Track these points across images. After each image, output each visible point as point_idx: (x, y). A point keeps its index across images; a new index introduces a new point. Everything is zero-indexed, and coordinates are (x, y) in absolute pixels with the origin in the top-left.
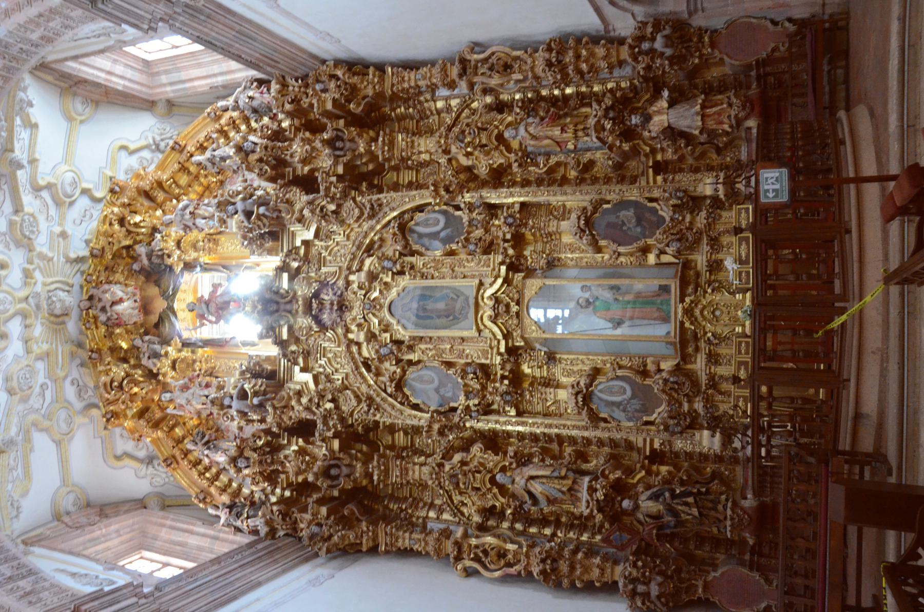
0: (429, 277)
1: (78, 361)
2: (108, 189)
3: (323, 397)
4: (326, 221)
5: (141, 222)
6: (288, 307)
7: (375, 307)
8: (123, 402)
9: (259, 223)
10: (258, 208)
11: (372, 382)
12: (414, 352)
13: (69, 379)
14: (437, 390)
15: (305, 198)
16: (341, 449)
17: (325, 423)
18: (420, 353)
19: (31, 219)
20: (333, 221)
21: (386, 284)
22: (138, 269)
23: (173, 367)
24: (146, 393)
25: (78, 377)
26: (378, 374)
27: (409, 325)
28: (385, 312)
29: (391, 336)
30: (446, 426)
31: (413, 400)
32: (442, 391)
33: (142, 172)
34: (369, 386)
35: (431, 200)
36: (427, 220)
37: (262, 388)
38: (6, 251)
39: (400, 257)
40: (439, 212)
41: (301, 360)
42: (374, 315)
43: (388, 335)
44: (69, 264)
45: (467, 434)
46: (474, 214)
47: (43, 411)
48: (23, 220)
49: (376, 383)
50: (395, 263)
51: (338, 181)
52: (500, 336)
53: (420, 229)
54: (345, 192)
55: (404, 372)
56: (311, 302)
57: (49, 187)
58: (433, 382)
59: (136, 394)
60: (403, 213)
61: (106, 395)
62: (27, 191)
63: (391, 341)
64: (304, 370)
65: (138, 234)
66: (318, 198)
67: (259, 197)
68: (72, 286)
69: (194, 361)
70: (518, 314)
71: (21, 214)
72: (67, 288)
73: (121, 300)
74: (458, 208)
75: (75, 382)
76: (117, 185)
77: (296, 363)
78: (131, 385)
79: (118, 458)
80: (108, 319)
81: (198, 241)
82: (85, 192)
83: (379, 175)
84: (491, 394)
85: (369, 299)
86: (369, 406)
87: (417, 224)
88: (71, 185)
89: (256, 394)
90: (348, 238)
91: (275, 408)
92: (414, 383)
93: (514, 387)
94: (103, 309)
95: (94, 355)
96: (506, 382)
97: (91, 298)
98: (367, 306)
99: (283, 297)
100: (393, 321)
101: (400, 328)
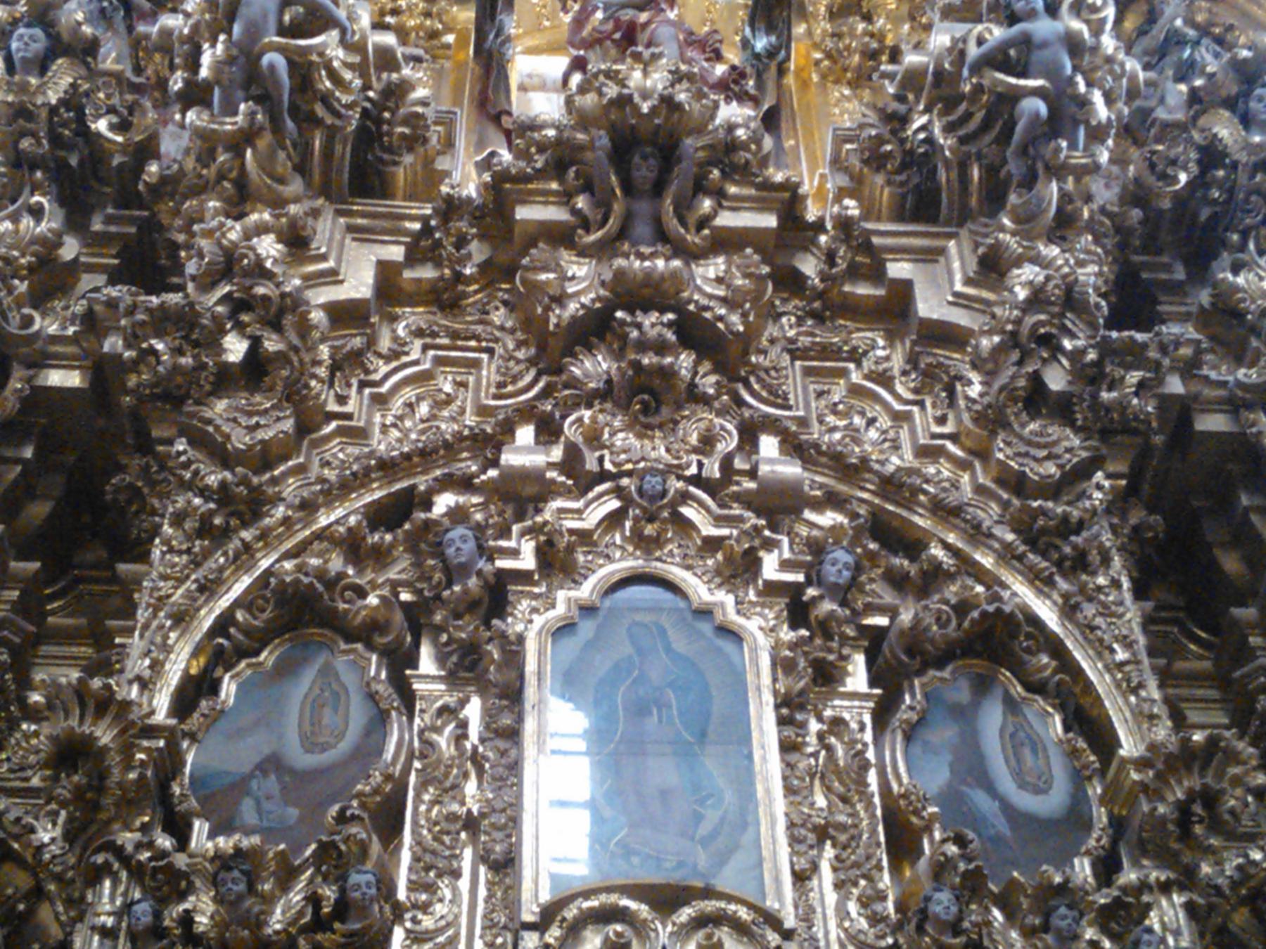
0: (789, 732)
3: (277, 327)
4: (997, 350)
6: (642, 229)
7: (651, 519)
9: (979, 116)
10: (1036, 92)
11: (323, 520)
12: (452, 679)
14: (273, 764)
15: (1090, 275)
16: (41, 398)
17: (162, 321)
18: (450, 700)
20: (1003, 379)
21: (751, 563)
26: (353, 547)
27: (572, 644)
29: (523, 577)
30: (98, 778)
31: (229, 688)
32: (272, 783)
34: (308, 507)
35: (1129, 747)
36: (1036, 745)
37: (320, 110)
39: (864, 630)
41: (427, 273)
42: (613, 520)
43: (527, 561)
45: (49, 916)
46: (1090, 934)
49: (319, 536)
50: (843, 594)
51: (1166, 402)
53: (992, 718)
54: (1127, 430)
55: (367, 633)
56: (662, 311)
58: (310, 744)
60: (1057, 648)
63: (505, 577)
64: (386, 271)
66: (1093, 325)
67: (1084, 103)
74: (1107, 867)
77: (412, 258)
81: (868, 18)
85: (685, 497)
86: (223, 495)
87: (1011, 705)
89: (302, 69)
90: (928, 453)
91: (241, 141)
92: (307, 679)
98: (653, 483)
99: (683, 208)
100: (586, 591)
101: (561, 609)
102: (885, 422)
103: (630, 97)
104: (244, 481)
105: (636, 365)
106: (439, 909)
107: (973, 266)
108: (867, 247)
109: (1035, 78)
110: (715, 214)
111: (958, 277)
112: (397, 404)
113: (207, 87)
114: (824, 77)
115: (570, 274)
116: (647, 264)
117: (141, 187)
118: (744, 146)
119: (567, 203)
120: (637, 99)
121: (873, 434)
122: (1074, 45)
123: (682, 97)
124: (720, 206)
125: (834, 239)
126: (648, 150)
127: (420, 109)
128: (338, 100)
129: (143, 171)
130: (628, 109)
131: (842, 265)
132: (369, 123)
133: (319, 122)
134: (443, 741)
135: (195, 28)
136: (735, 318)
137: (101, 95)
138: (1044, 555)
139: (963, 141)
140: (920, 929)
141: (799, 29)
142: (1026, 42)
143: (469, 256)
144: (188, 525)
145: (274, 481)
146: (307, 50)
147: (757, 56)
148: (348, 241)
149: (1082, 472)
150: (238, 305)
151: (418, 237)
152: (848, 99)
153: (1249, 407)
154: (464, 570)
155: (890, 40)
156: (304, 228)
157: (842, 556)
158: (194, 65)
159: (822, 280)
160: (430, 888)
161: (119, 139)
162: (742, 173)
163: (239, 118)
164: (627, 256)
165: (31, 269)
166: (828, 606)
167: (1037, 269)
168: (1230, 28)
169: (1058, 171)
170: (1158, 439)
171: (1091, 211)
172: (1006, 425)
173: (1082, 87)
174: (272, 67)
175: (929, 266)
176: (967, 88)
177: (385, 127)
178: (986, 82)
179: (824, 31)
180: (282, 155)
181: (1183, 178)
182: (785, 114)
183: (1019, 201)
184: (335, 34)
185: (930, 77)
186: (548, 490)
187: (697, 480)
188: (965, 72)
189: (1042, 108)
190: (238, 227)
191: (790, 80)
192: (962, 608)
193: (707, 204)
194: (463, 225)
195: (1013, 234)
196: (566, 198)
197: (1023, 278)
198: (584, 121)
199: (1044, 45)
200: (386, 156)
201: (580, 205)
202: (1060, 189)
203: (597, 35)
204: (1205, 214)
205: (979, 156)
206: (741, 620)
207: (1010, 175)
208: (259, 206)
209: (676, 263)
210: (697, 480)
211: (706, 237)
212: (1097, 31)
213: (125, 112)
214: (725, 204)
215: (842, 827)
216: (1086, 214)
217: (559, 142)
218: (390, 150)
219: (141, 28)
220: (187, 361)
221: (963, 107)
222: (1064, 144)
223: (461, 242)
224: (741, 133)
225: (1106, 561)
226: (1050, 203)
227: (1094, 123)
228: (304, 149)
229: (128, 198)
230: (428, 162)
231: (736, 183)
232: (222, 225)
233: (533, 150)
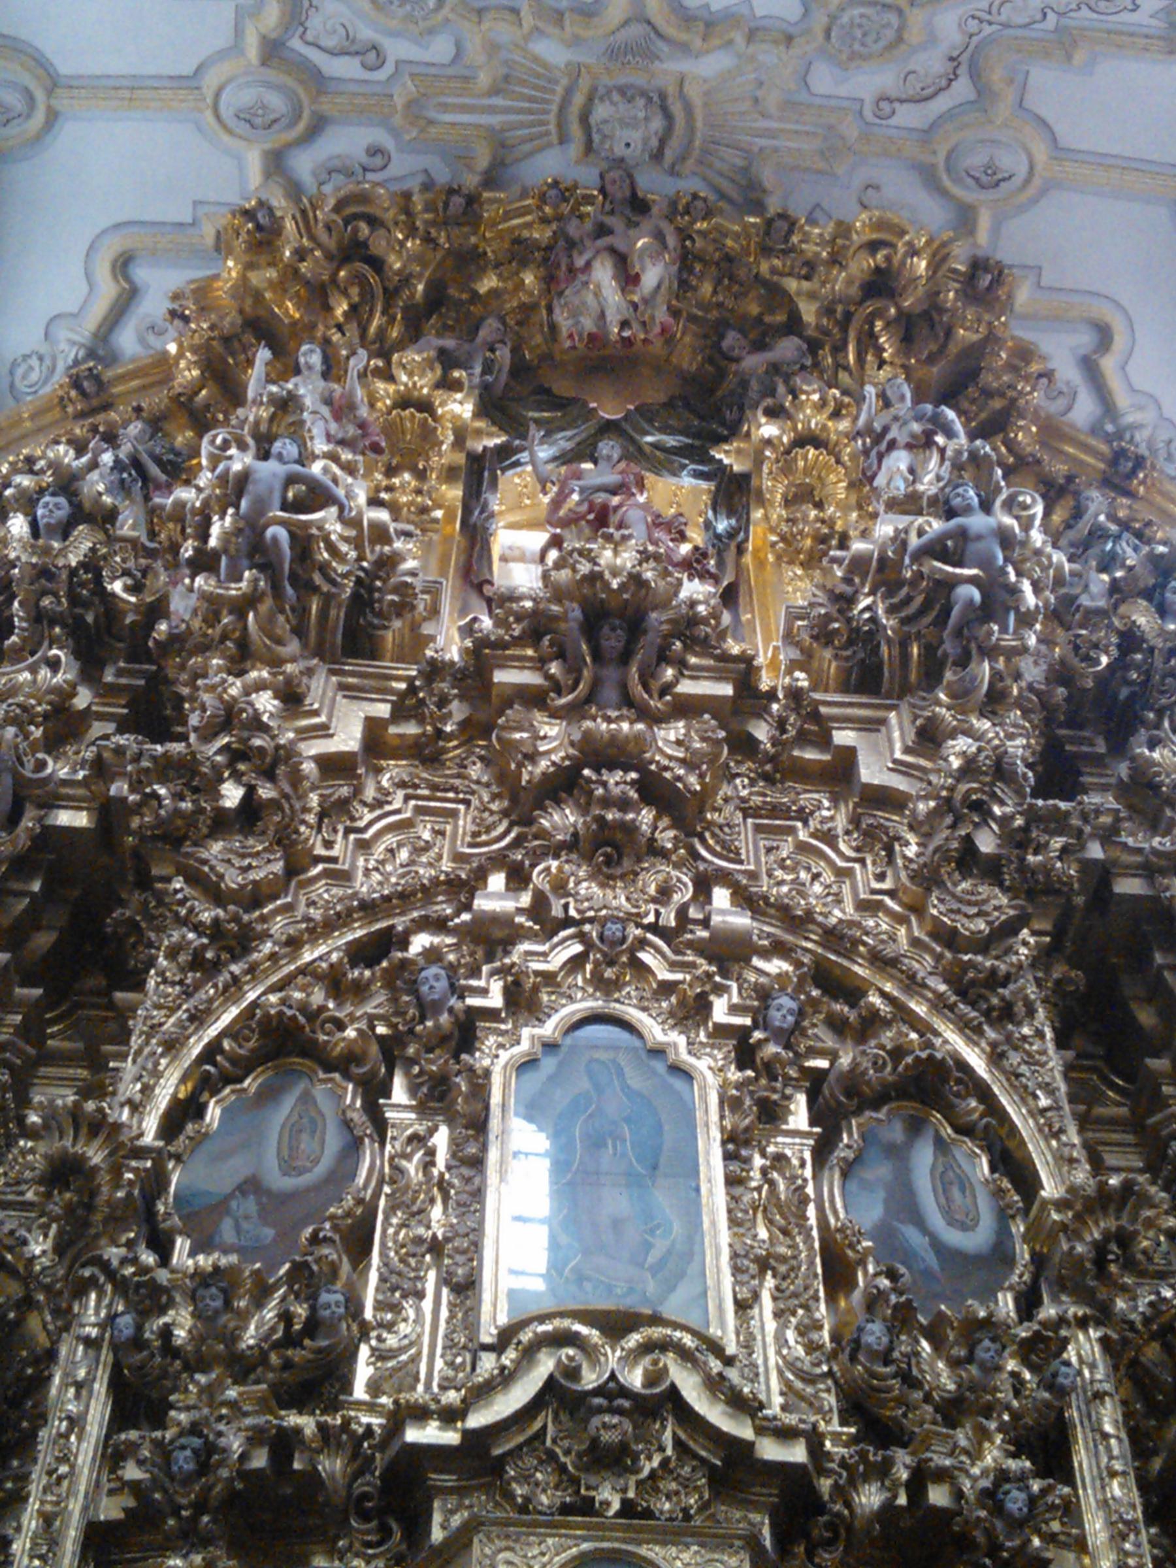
0: (734, 1167)
1: (443, 175)
2: (980, 253)
3: (269, 775)
4: (932, 814)
5: (880, 350)
6: (610, 693)
7: (611, 963)
8: (301, 254)
9: (919, 600)
10: (972, 580)
11: (307, 956)
12: (422, 1109)
13: (389, 144)
14: (251, 1186)
15: (1017, 747)
16: (50, 836)
17: (166, 769)
18: (420, 1128)
19: (890, 34)
20: (938, 840)
21: (702, 1006)
22: (725, 344)
23: (404, 402)
24: (326, 342)
25: (394, 170)
26: (335, 982)
27: (535, 1080)
28: (584, 1004)
29: (491, 1014)
31: (213, 1113)
32: (250, 1205)
33: (1034, 368)
34: (294, 944)
35: (1050, 1189)
36: (964, 1184)
37: (317, 578)
40: (1003, 1232)
41: (411, 729)
42: (576, 963)
43: (495, 999)
44: (740, 162)
45: (37, 1325)
46: (1011, 1365)
49: (302, 971)
50: (787, 1038)
51: (1087, 866)
52: (477, 1420)
53: (924, 1156)
55: (345, 1063)
56: (626, 770)
58: (289, 1167)
59: (328, 309)
60: (984, 1093)
61: (332, 202)
62: (973, 25)
64: (373, 726)
65: (839, 349)
66: (1020, 793)
67: (1015, 591)
68: (673, 172)
69: (421, 475)
70: (588, 1507)
72: (669, 155)
73: (628, 279)
74: (1028, 1303)
75: (378, 161)
76: (998, 281)
78: (354, 291)
79: (123, 265)
80: (571, 244)
81: (819, 505)
82: (965, 218)
83: (1108, 1058)
84: (209, 1392)
85: (642, 943)
86: (216, 931)
87: (941, 1145)
88: (990, 168)
89: (303, 542)
90: (868, 907)
91: (241, 607)
92: (288, 1103)
93: (232, 1498)
94: (602, 230)
95: (457, 201)
96: (260, 1460)
97: (639, 206)
98: (613, 929)
100: (549, 1028)
101: (525, 1045)
102: (828, 877)
103: (600, 575)
104: (236, 919)
105: (601, 820)
106: (404, 1328)
107: (911, 736)
108: (815, 716)
109: (970, 567)
110: (676, 682)
111: (898, 746)
112: (379, 850)
113: (215, 555)
114: (779, 558)
115: (542, 734)
116: (613, 726)
117: (151, 644)
118: (704, 621)
119: (540, 669)
120: (607, 575)
121: (817, 888)
122: (1005, 539)
123: (649, 575)
124: (682, 674)
125: (786, 707)
126: (617, 622)
127: (409, 579)
128: (335, 571)
129: (152, 629)
130: (598, 584)
131: (792, 732)
132: (362, 591)
133: (316, 589)
134: (412, 1167)
135: (206, 503)
136: (693, 780)
137: (118, 559)
138: (973, 1004)
139: (905, 621)
140: (853, 1359)
141: (757, 514)
142: (962, 534)
143: (450, 713)
144: (182, 958)
145: (263, 919)
146: (307, 525)
147: (718, 537)
148: (338, 698)
149: (1010, 929)
150: (236, 755)
151: (403, 695)
152: (800, 578)
153: (1163, 872)
154: (436, 1007)
155: (839, 526)
156: (299, 685)
157: (786, 1002)
158: (204, 536)
159: (773, 745)
160: (396, 1308)
161: (133, 599)
162: (703, 645)
163: (244, 585)
164: (594, 719)
165: (46, 716)
166: (772, 1049)
167: (970, 741)
168: (1149, 524)
169: (990, 652)
170: (1079, 900)
171: (1020, 689)
172: (940, 884)
173: (1013, 577)
174: (275, 539)
175: (874, 735)
176: (909, 575)
177: (377, 595)
178: (925, 570)
179: (780, 516)
180: (281, 618)
181: (1104, 660)
182: (743, 589)
183: (955, 678)
184: (334, 510)
185: (874, 563)
186: (516, 935)
187: (654, 928)
188: (907, 561)
189: (977, 595)
190: (239, 684)
191: (748, 559)
192: (897, 1053)
193: (670, 672)
194: (444, 686)
195: (949, 709)
196: (540, 663)
197: (957, 749)
198: (558, 594)
199: (979, 537)
200: (376, 621)
201: (553, 671)
202: (992, 668)
203: (572, 516)
204: (1124, 693)
205: (919, 636)
206: (692, 1060)
207: (946, 655)
208: (259, 665)
209: (640, 726)
210: (654, 928)
211: (667, 704)
212: (1027, 526)
213: (139, 575)
214: (686, 673)
215: (783, 1259)
216: (1015, 692)
217: (535, 613)
218: (380, 615)
219: (158, 500)
220: (186, 805)
221: (904, 591)
222: (996, 628)
223: (443, 702)
224: (702, 609)
225: (1031, 1012)
226: (982, 681)
227: (1023, 609)
228: (302, 611)
229: (138, 651)
230: (415, 627)
231: (696, 655)
232: (224, 681)
233: (511, 619)
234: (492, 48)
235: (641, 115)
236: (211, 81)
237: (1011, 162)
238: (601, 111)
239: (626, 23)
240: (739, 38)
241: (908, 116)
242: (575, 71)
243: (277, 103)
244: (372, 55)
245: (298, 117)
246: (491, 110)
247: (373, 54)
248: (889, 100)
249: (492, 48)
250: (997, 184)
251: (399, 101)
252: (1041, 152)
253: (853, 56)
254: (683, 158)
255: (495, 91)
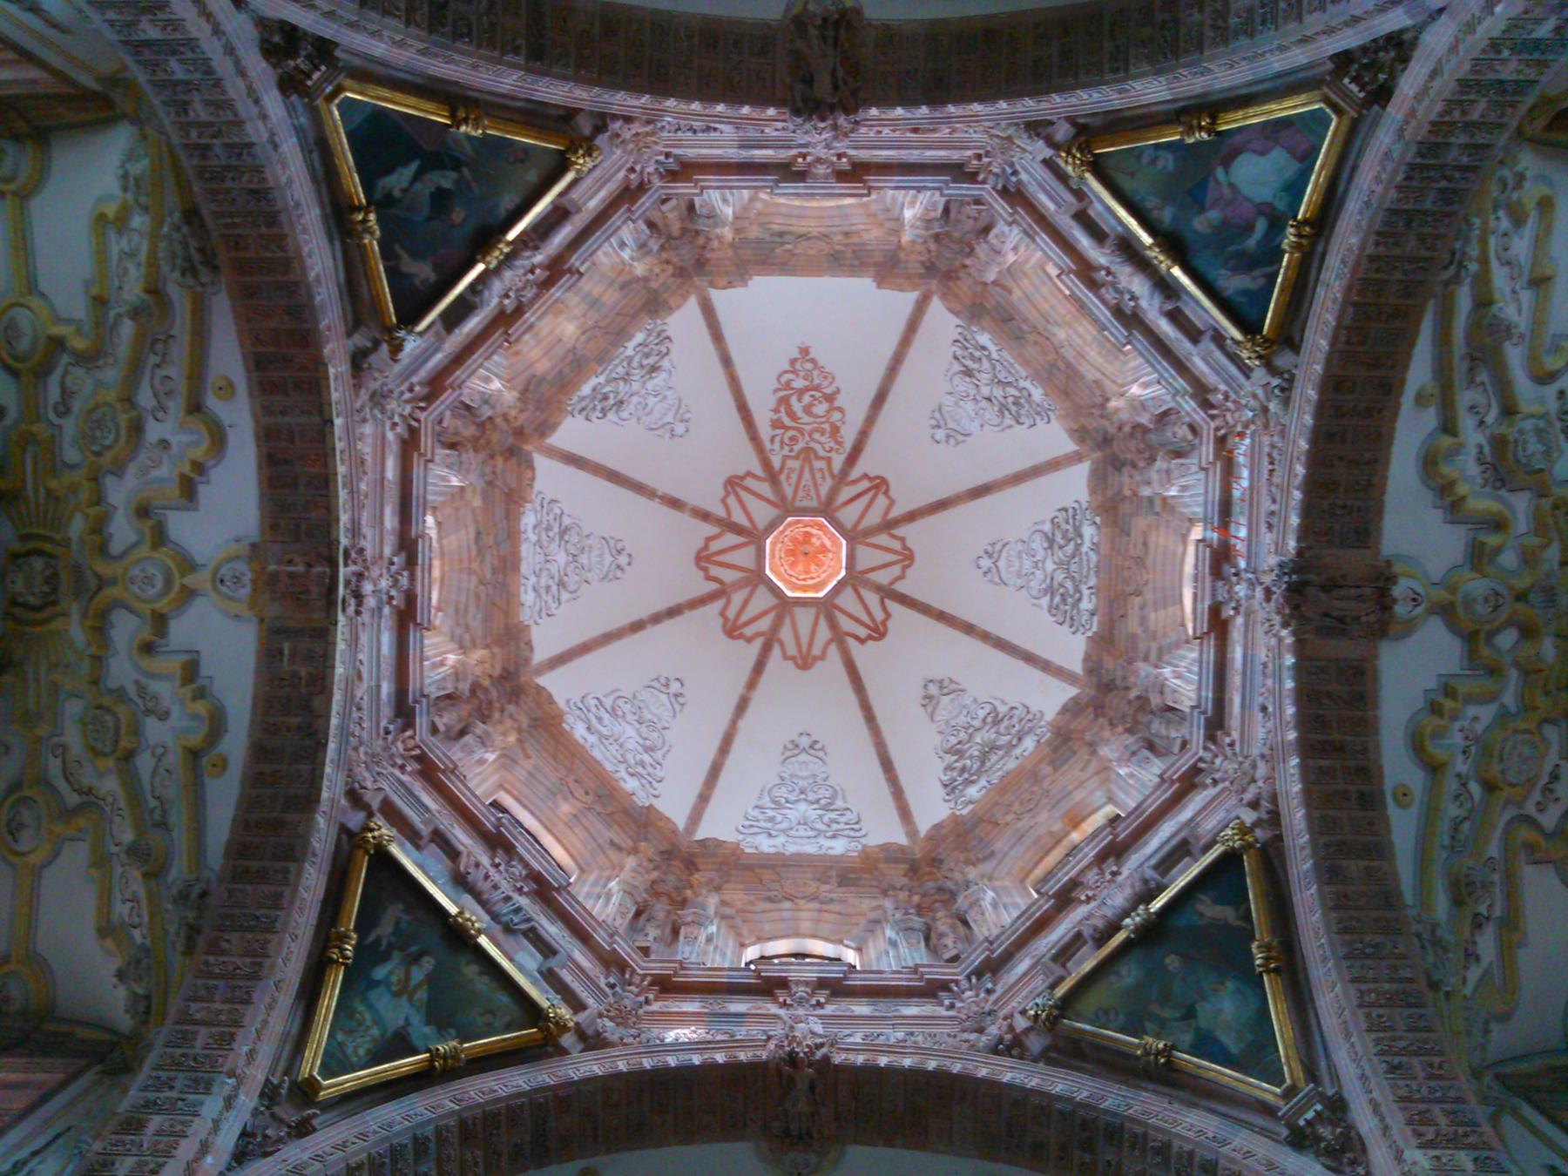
19: (99, 746)
38: (143, 680)
47: (65, 359)
48: (116, 742)
57: (67, 814)
71: (119, 754)
72: (17, 611)
88: (22, 826)
234: (74, 488)
235: (36, 590)
236: (34, 302)
237: (26, 841)
238: (38, 564)
239: (96, 574)
240: (93, 650)
241: (54, 766)
242: (66, 543)
243: (23, 345)
244: (62, 409)
245: (16, 359)
246: (36, 491)
247: (64, 410)
248: (63, 754)
249: (74, 488)
250: (10, 833)
251: (35, 428)
252: (35, 858)
253: (85, 725)
254: (16, 620)
255: (49, 493)
